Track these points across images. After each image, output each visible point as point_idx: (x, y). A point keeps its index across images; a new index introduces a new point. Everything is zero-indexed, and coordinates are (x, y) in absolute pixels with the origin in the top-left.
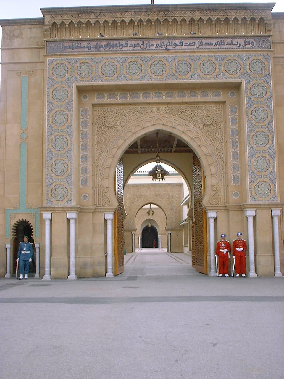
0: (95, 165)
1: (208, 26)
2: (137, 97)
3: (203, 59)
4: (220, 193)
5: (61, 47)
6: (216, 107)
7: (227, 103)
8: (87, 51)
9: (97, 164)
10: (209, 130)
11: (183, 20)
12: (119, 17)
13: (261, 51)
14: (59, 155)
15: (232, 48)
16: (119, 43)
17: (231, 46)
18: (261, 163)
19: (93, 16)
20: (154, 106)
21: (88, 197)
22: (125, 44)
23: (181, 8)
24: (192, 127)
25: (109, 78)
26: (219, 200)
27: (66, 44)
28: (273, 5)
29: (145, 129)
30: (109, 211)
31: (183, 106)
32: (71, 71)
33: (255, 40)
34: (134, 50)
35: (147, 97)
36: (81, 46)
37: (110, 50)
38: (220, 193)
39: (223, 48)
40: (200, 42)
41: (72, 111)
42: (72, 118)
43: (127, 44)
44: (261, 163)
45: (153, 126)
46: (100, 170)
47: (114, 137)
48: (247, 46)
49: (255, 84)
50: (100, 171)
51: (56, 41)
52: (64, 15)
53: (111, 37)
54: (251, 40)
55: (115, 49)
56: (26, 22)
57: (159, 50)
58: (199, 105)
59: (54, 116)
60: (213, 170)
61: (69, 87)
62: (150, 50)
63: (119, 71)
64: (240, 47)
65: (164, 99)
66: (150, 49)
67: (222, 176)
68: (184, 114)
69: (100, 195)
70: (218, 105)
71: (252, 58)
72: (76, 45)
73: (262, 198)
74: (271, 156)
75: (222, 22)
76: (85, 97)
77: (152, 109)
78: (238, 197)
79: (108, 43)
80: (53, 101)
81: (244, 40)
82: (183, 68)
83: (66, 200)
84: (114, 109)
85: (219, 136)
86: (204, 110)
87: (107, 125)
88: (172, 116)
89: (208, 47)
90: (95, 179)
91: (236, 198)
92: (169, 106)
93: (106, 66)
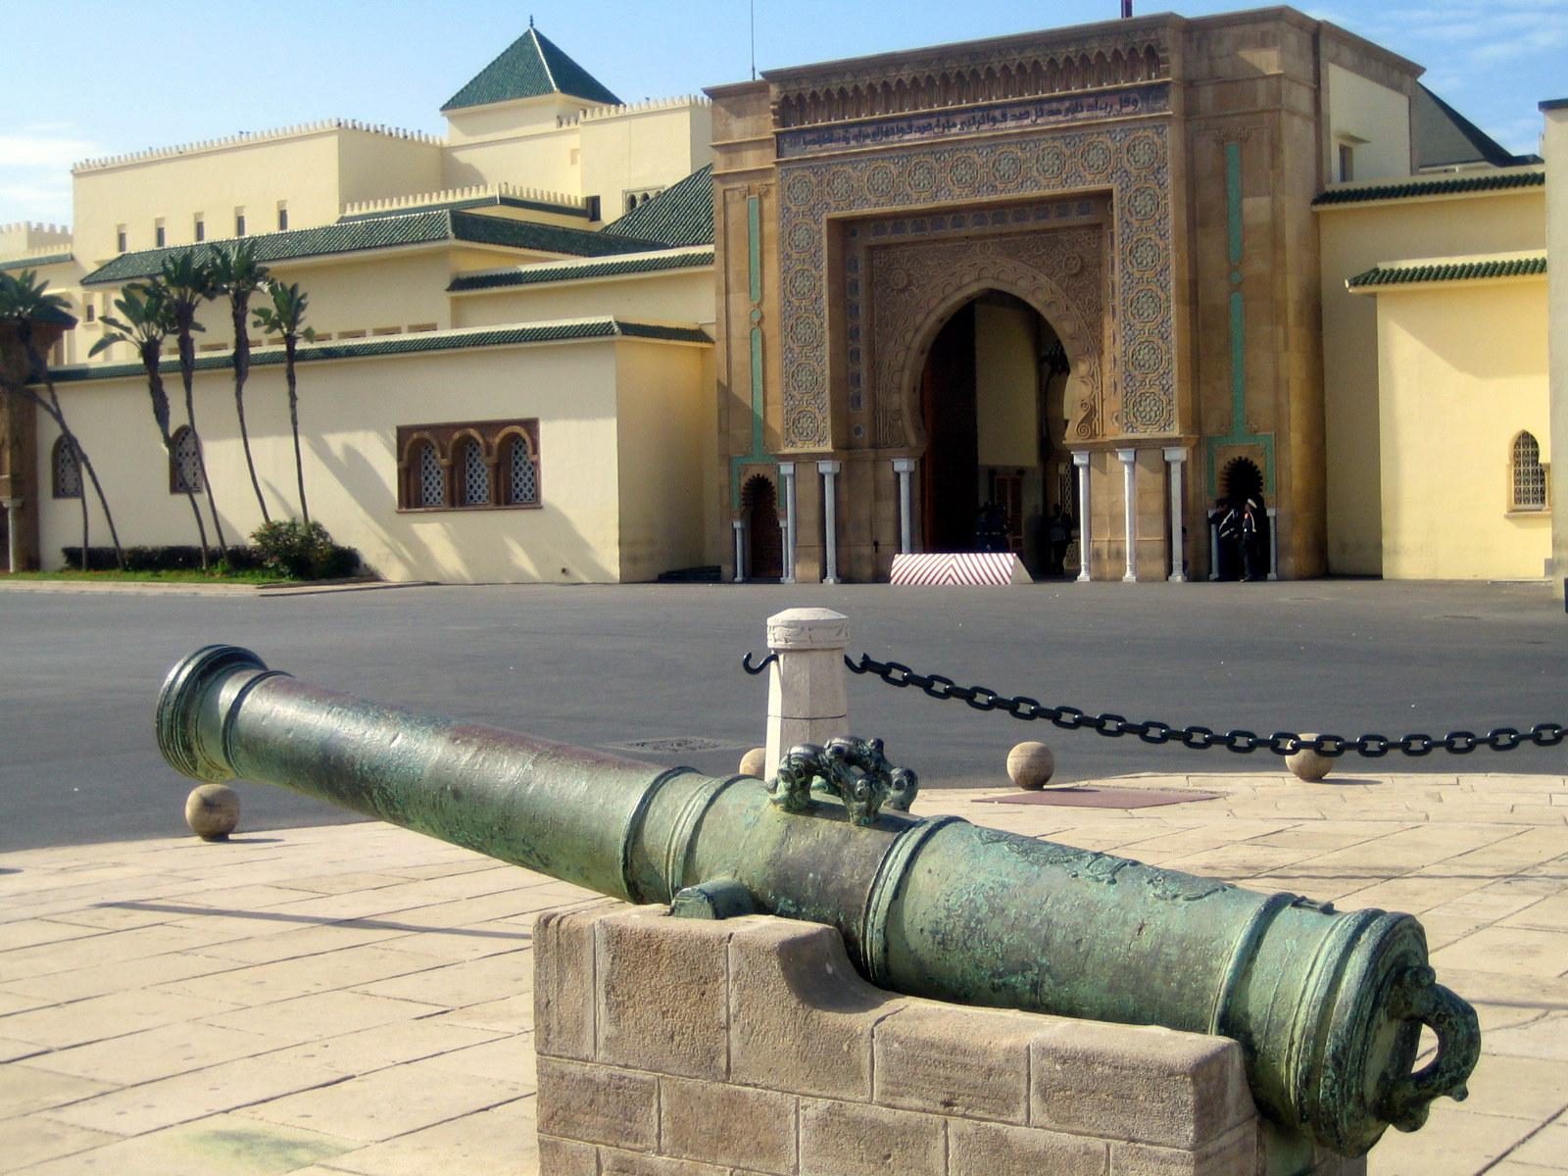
0: (874, 368)
12: (892, 76)
19: (848, 78)
24: (1043, 279)
48: (1124, 110)
49: (1138, 190)
61: (816, 222)
62: (950, 135)
65: (990, 228)
76: (853, 234)
89: (1052, 119)
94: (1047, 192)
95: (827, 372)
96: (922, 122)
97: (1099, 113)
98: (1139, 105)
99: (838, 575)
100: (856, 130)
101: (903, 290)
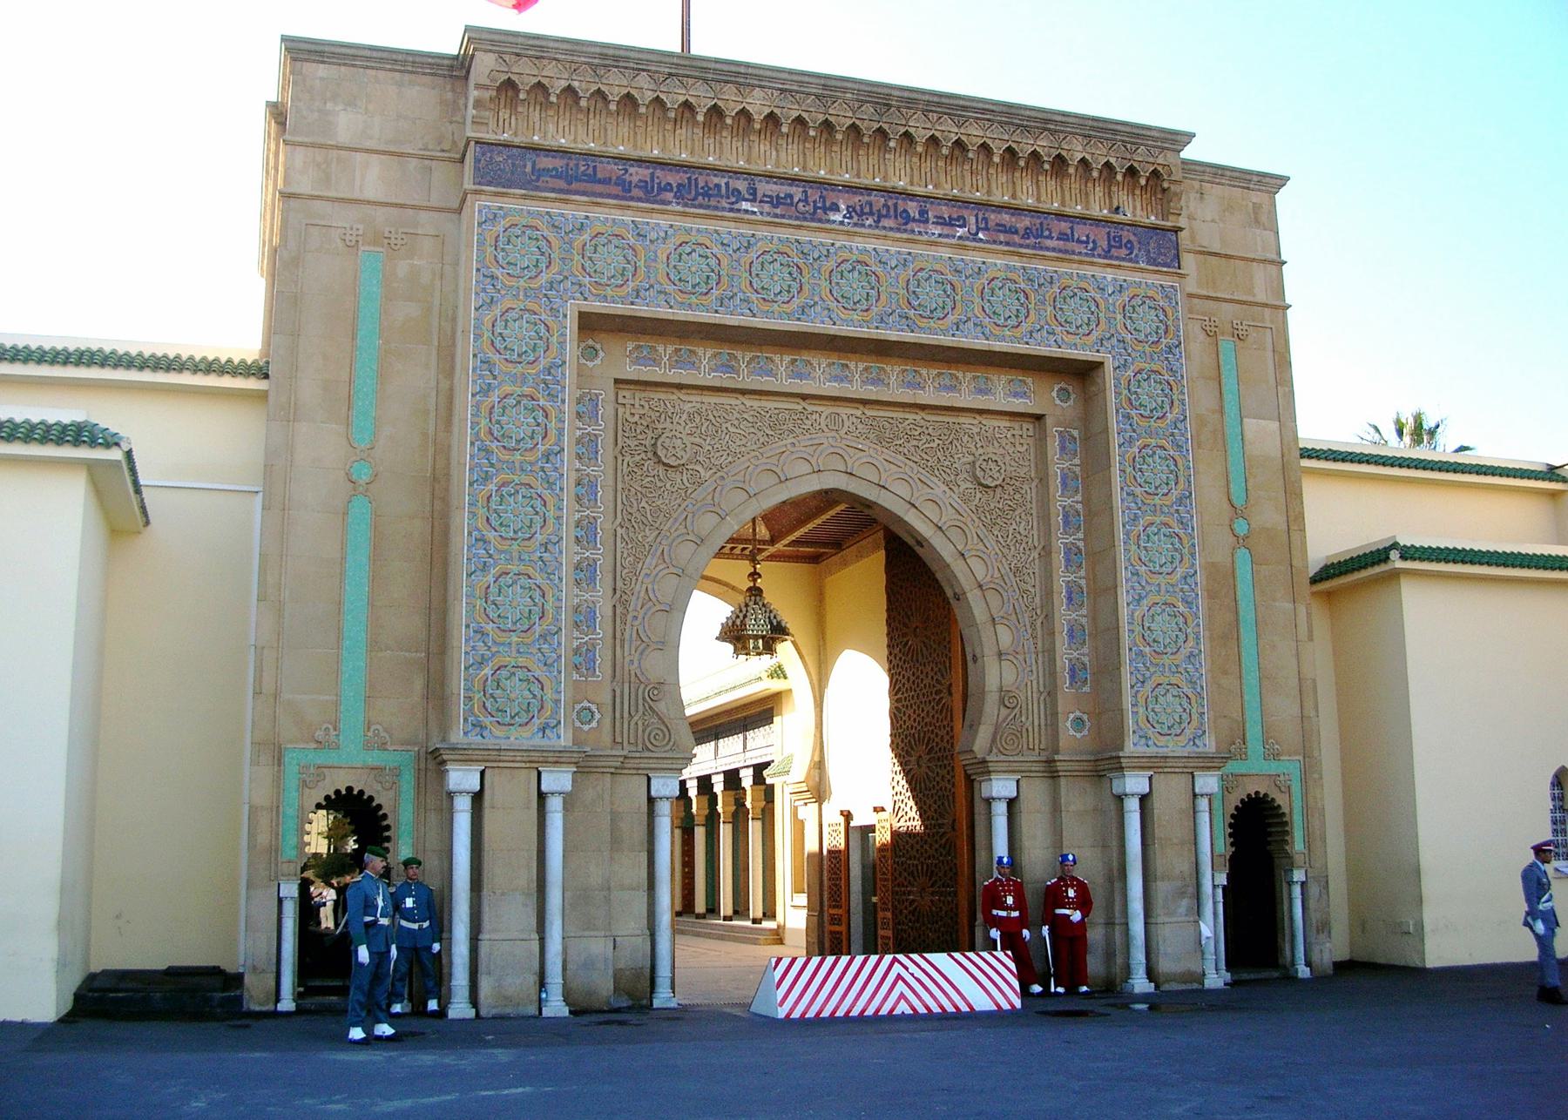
2: (770, 373)
3: (990, 275)
5: (529, 169)
12: (731, 101)
13: (1156, 272)
14: (515, 555)
16: (727, 184)
17: (1070, 245)
19: (643, 80)
20: (819, 409)
21: (597, 716)
24: (939, 489)
25: (693, 299)
27: (546, 162)
28: (1191, 136)
31: (911, 417)
35: (800, 376)
36: (599, 175)
41: (563, 401)
44: (1162, 625)
48: (1114, 252)
52: (545, 62)
53: (693, 160)
55: (713, 202)
60: (1005, 637)
61: (554, 312)
63: (725, 279)
70: (1016, 425)
71: (1132, 291)
74: (1188, 603)
75: (1047, 166)
78: (1086, 732)
80: (496, 358)
82: (930, 294)
89: (1002, 237)
91: (1078, 735)
92: (869, 413)
93: (684, 256)
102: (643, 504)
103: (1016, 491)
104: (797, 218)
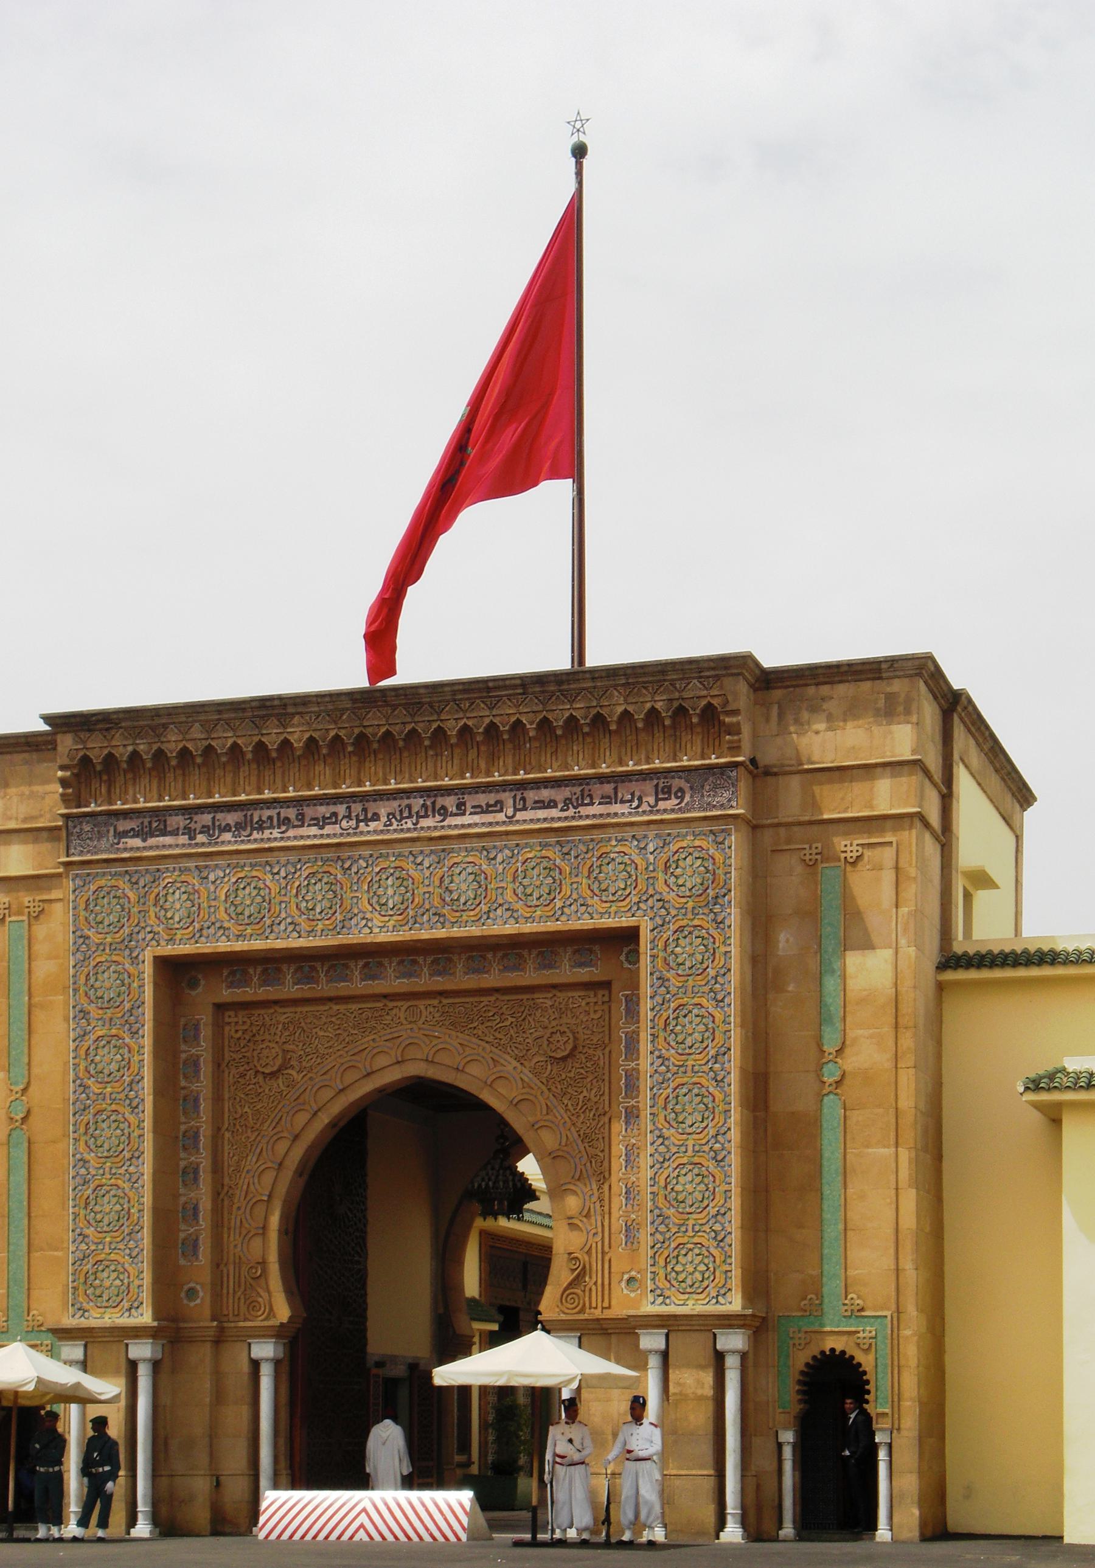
1: (548, 740)
4: (590, 1277)
6: (588, 1000)
7: (615, 987)
8: (184, 845)
9: (231, 1192)
10: (564, 1077)
11: (465, 730)
15: (616, 814)
16: (279, 814)
18: (686, 1184)
19: (196, 732)
20: (399, 1004)
21: (201, 1294)
22: (297, 819)
23: (454, 693)
24: (510, 1065)
26: (587, 1299)
29: (373, 1076)
30: (262, 1334)
32: (140, 912)
33: (688, 781)
34: (322, 836)
35: (373, 977)
37: (252, 838)
38: (590, 1277)
39: (587, 817)
40: (518, 798)
42: (140, 1058)
43: (301, 817)
44: (686, 1184)
45: (397, 1066)
46: (239, 1208)
47: (280, 1107)
48: (662, 805)
49: (681, 929)
50: (240, 1212)
51: (92, 815)
54: (677, 783)
56: (17, 744)
57: (395, 830)
58: (536, 996)
59: (92, 1052)
61: (135, 960)
64: (640, 810)
65: (425, 981)
66: (369, 829)
67: (599, 1224)
68: (489, 1024)
69: (239, 1286)
70: (592, 994)
72: (155, 825)
73: (687, 1296)
76: (193, 984)
77: (394, 1012)
79: (245, 816)
81: (655, 782)
83: (126, 1304)
84: (284, 1015)
85: (593, 1092)
86: (550, 1011)
87: (261, 1070)
88: (454, 1033)
89: (541, 814)
90: (226, 1236)
92: (445, 1001)
94: (528, 928)
95: (147, 1200)
96: (323, 810)
97: (617, 808)
98: (687, 799)
99: (155, 1520)
100: (206, 818)
101: (273, 1075)
102: (246, 1109)
103: (588, 1059)
104: (341, 835)
